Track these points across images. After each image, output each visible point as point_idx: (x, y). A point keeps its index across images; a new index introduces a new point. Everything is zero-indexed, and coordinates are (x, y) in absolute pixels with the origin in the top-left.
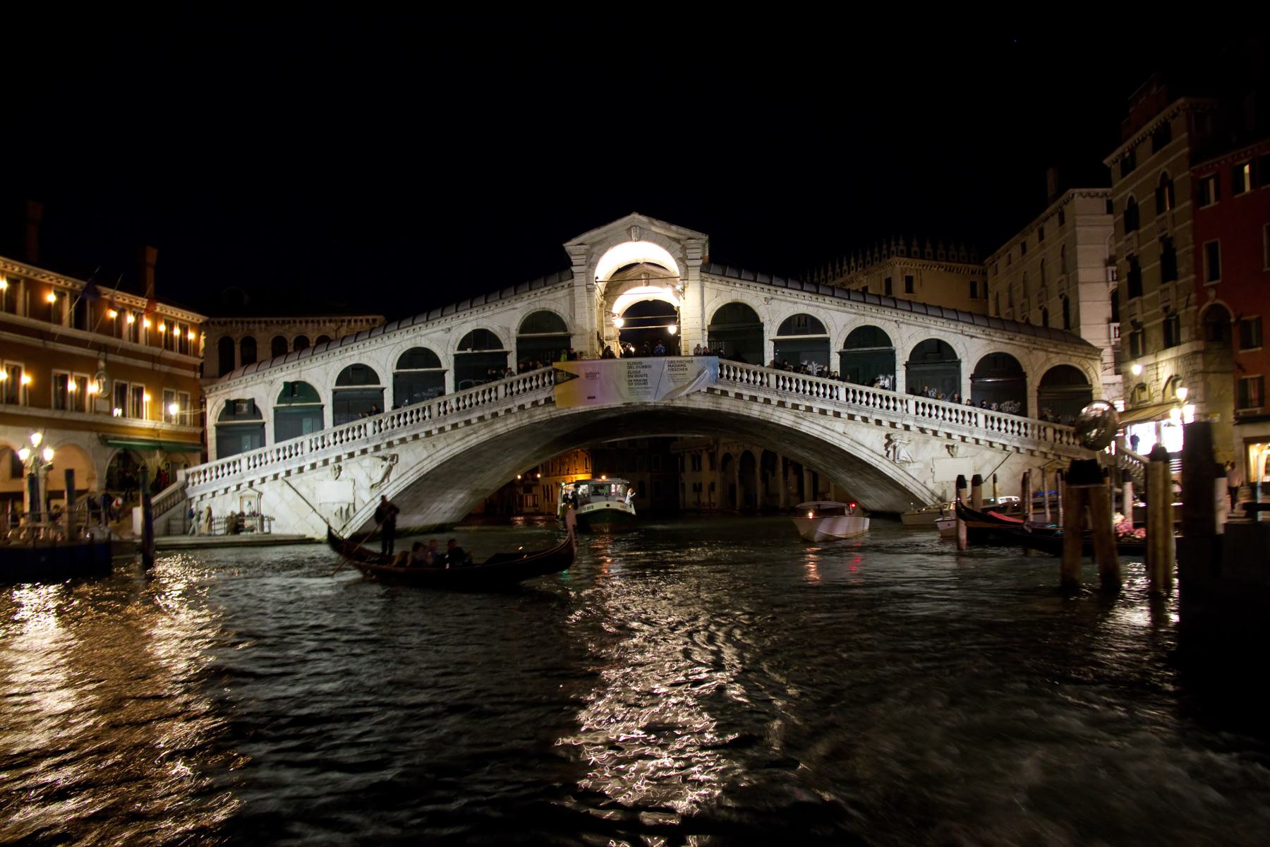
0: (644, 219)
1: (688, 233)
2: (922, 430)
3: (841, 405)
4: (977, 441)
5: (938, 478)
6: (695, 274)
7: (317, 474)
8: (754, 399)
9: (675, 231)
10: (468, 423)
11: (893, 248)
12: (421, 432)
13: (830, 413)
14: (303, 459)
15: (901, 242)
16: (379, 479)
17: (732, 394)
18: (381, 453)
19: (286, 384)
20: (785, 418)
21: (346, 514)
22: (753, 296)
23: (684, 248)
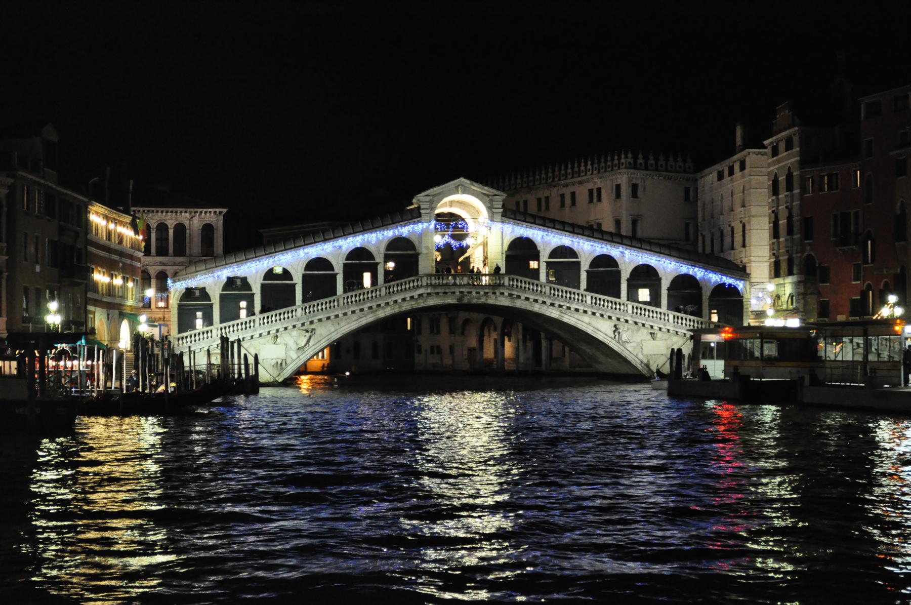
0: (467, 181)
1: (495, 192)
2: (636, 323)
3: (588, 307)
4: (668, 331)
5: (645, 352)
6: (499, 217)
7: (262, 340)
8: (536, 301)
9: (486, 190)
10: (362, 310)
11: (623, 161)
12: (332, 315)
13: (581, 311)
14: (255, 330)
15: (630, 155)
16: (303, 344)
17: (523, 298)
18: (304, 328)
19: (229, 278)
20: (554, 313)
21: (281, 365)
22: (536, 234)
23: (491, 201)
